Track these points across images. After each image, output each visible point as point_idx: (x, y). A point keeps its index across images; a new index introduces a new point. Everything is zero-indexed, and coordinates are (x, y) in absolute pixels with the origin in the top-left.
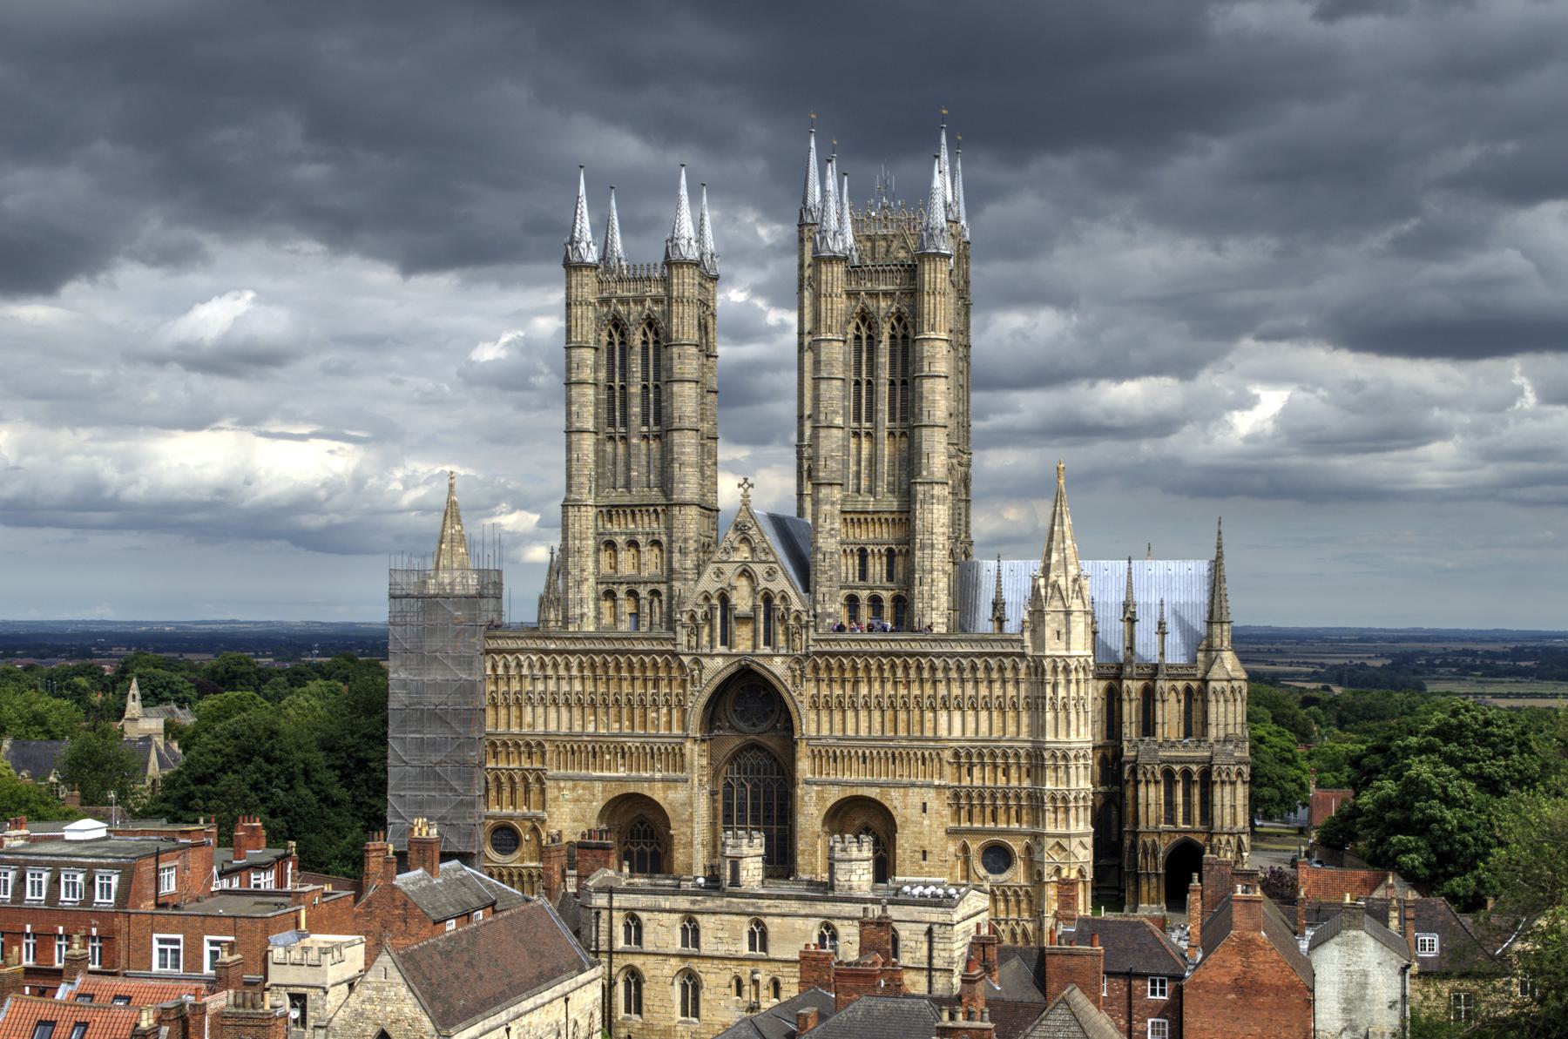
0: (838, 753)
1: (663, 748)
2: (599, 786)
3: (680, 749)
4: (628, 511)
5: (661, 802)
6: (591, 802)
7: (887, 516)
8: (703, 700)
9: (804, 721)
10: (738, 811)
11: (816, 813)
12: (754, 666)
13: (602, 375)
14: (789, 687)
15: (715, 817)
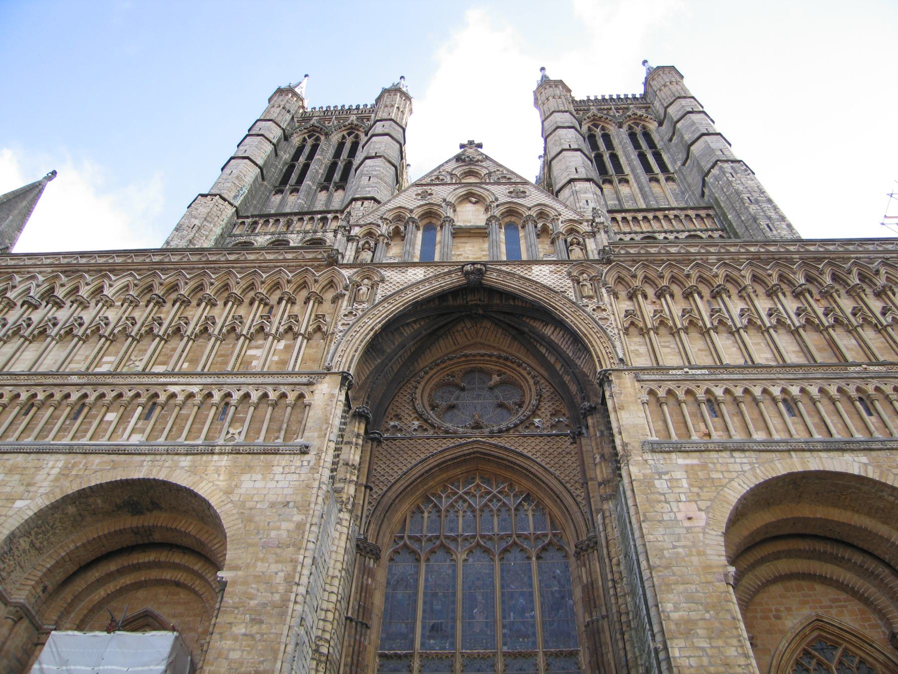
0: (719, 392)
1: (255, 396)
2: (54, 464)
3: (301, 396)
4: (283, 220)
5: (213, 502)
6: (13, 500)
7: (676, 212)
8: (373, 322)
9: (617, 344)
10: (429, 611)
11: (701, 519)
12: (492, 278)
13: (286, 156)
14: (574, 300)
15: (364, 609)
